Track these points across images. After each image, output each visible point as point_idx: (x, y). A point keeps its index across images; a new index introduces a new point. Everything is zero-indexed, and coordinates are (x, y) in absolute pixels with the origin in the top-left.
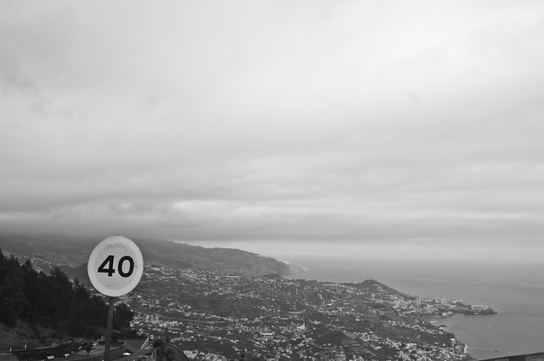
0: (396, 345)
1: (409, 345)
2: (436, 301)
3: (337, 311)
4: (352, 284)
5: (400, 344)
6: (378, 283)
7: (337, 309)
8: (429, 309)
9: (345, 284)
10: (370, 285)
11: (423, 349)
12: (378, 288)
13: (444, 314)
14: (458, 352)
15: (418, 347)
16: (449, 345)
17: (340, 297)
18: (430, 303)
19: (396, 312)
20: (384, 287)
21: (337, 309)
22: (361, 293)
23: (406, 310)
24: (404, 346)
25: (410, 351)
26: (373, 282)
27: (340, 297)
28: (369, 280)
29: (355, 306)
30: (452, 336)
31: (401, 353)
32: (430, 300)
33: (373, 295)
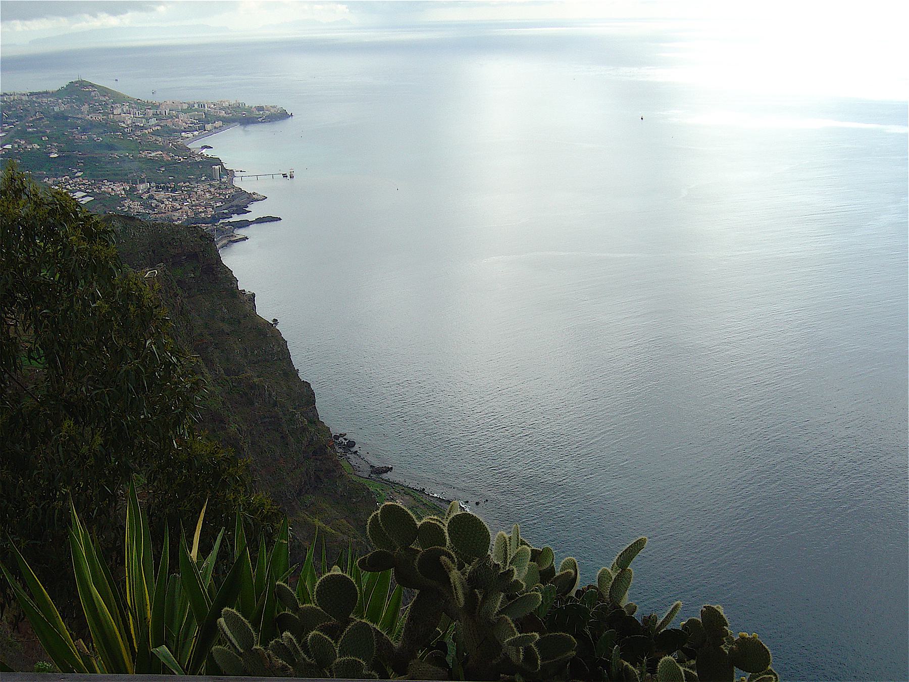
0: (119, 189)
1: (142, 187)
2: (196, 106)
3: (16, 146)
4: (47, 93)
5: (128, 188)
6: (93, 86)
7: (16, 142)
8: (183, 120)
9: (32, 94)
10: (78, 90)
11: (165, 189)
12: (93, 94)
13: (209, 127)
14: (223, 187)
15: (157, 187)
16: (211, 177)
17: (20, 118)
18: (184, 111)
19: (124, 134)
20: (105, 91)
21: (16, 142)
22: (63, 107)
23: (143, 128)
24: (133, 189)
25: (145, 196)
26: (82, 84)
27: (20, 118)
28: (76, 82)
29: (48, 131)
30: (218, 162)
31: (127, 203)
32: (185, 106)
33: (85, 108)
